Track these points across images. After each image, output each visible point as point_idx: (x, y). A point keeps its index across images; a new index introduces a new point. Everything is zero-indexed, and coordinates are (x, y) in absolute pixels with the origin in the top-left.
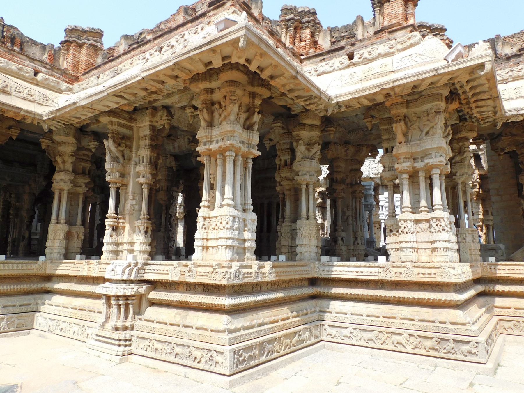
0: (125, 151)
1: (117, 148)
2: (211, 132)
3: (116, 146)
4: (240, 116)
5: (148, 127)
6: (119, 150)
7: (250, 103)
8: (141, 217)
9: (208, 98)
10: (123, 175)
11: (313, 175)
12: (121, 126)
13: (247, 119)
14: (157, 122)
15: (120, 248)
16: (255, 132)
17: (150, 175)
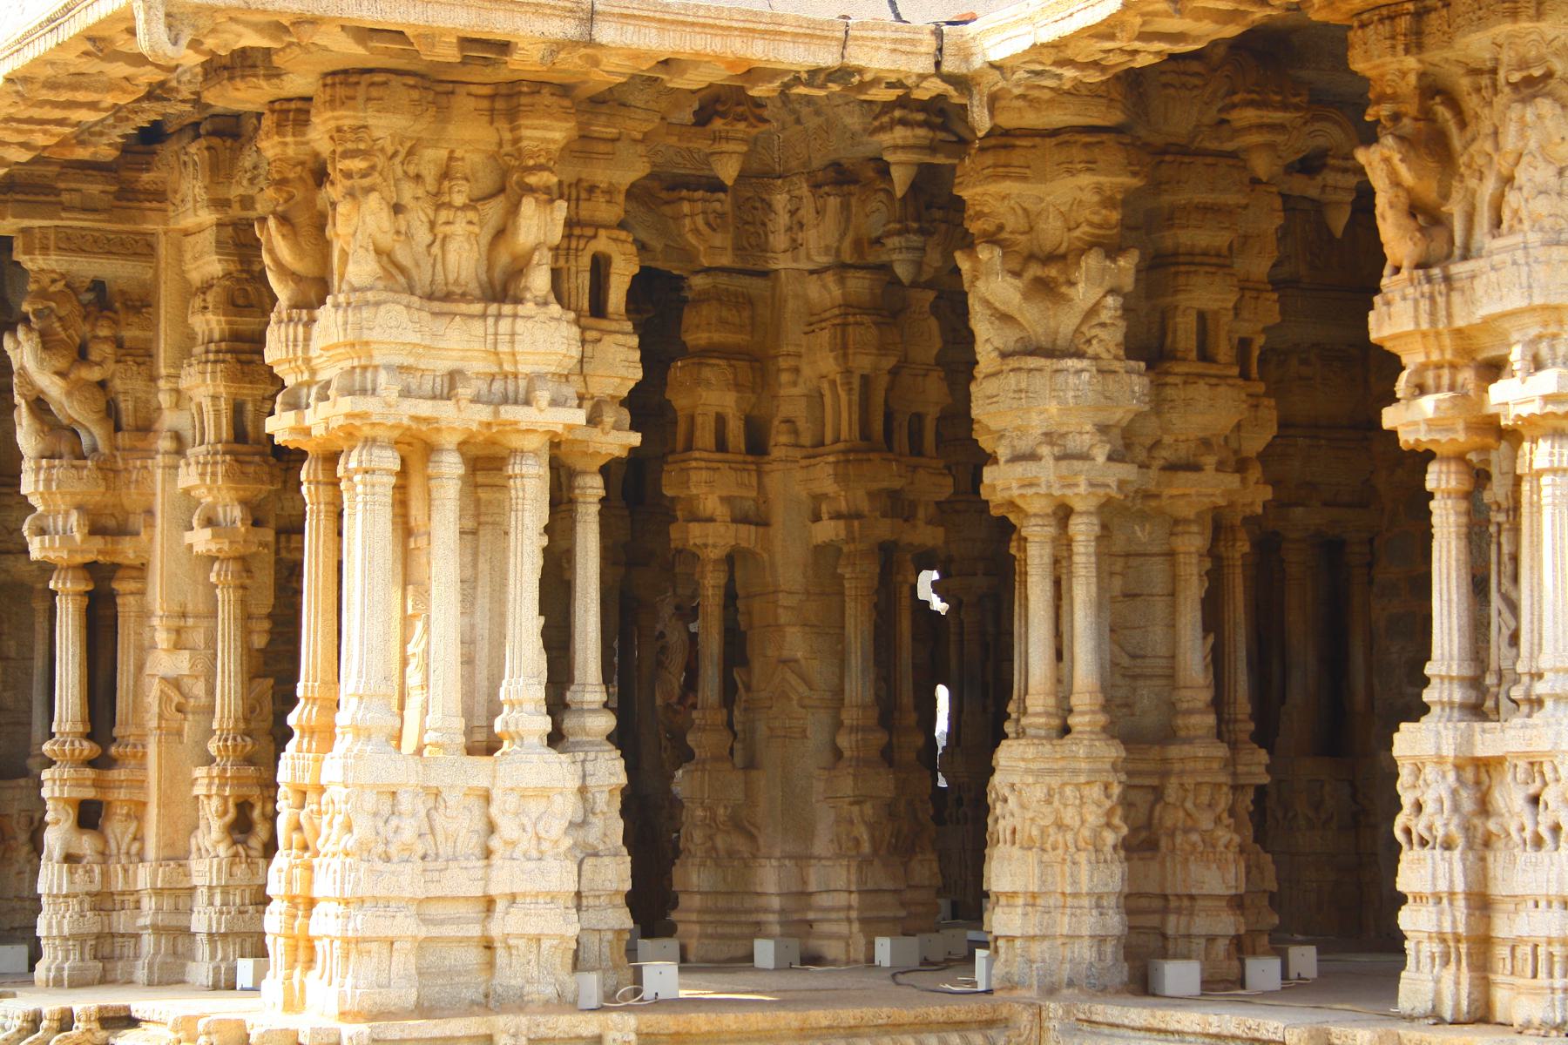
0: (118, 384)
1: (62, 374)
2: (307, 339)
3: (61, 364)
4: (441, 230)
5: (209, 236)
6: (88, 384)
7: (500, 144)
8: (213, 747)
9: (291, 151)
10: (106, 525)
11: (1084, 457)
12: (81, 251)
13: (501, 233)
14: (247, 202)
15: (121, 922)
16: (528, 308)
17: (237, 512)
